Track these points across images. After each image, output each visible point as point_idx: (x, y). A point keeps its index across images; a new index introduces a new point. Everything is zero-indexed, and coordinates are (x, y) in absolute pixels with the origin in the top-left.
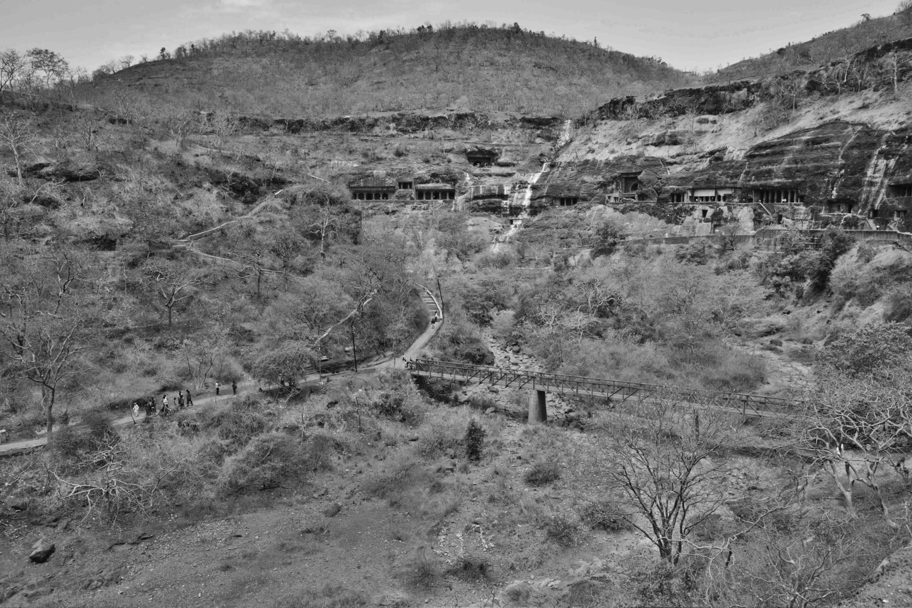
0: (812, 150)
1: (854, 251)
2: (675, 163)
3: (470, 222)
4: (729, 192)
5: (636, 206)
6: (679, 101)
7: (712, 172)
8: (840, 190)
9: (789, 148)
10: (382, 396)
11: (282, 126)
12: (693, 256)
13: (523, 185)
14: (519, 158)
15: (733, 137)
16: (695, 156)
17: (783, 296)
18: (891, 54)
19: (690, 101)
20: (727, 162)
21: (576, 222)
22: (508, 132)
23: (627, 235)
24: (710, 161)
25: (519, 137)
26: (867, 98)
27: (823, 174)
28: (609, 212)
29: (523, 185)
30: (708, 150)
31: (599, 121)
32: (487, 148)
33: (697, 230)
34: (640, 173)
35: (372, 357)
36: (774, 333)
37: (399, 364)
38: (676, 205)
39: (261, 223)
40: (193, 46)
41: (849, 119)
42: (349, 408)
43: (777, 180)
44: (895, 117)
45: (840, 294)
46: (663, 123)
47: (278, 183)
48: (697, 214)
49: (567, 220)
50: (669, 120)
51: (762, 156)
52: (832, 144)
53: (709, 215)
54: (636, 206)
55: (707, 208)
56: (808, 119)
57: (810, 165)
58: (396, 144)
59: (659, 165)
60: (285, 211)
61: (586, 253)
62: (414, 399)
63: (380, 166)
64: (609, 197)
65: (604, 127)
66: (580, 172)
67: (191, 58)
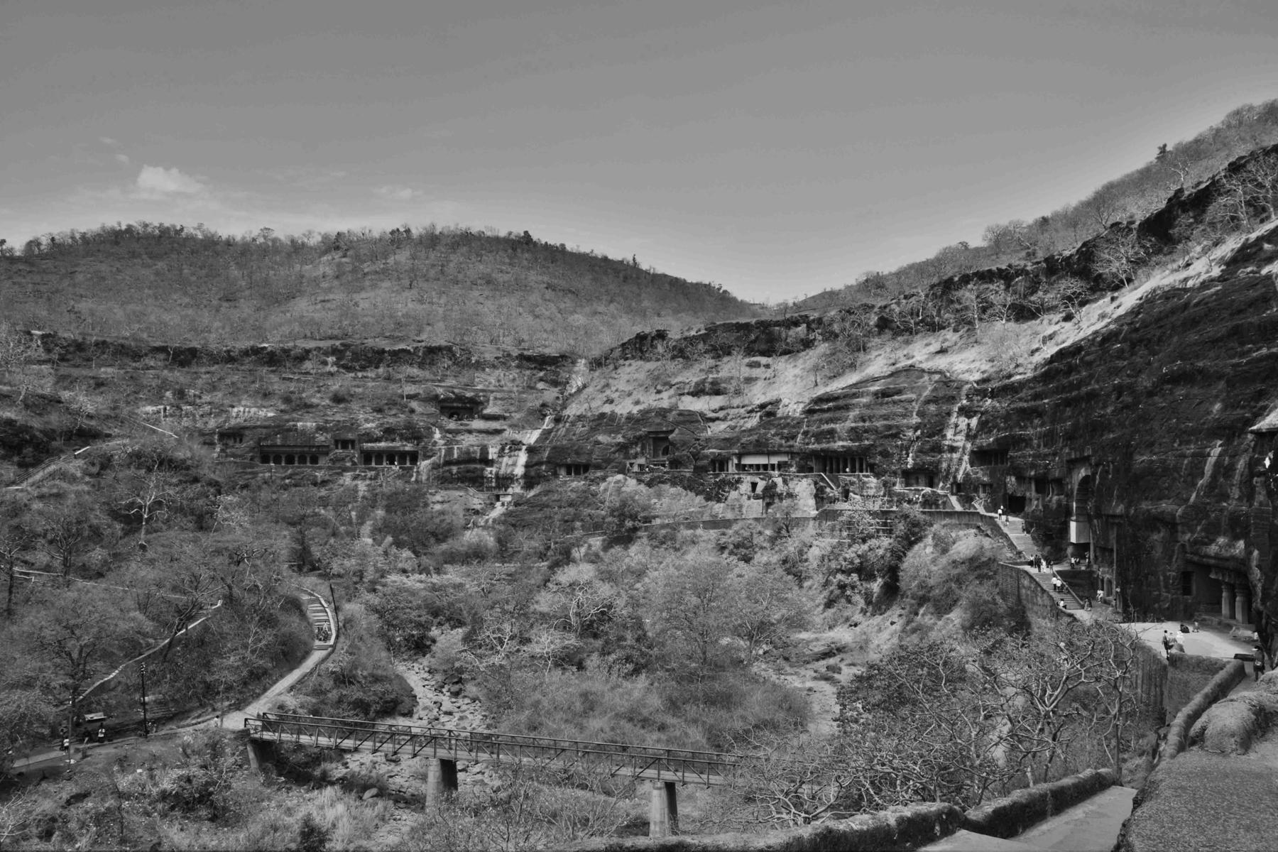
0: (881, 404)
1: (929, 540)
2: (718, 419)
3: (438, 498)
4: (784, 459)
5: (667, 476)
6: (723, 338)
7: (762, 431)
9: (855, 401)
10: (180, 778)
11: (162, 356)
12: (737, 546)
13: (516, 445)
14: (513, 409)
15: (790, 385)
16: (742, 411)
17: (849, 602)
18: (969, 286)
19: (738, 339)
21: (587, 498)
22: (499, 372)
23: (654, 517)
25: (514, 380)
26: (946, 340)
27: (896, 436)
28: (631, 484)
29: (516, 445)
30: (758, 402)
31: (621, 362)
32: (469, 395)
33: (744, 510)
34: (672, 431)
35: (190, 711)
36: (834, 655)
37: (234, 722)
38: (717, 476)
39: (41, 497)
40: (53, 239)
41: (925, 366)
42: (110, 802)
43: (841, 443)
44: (977, 364)
45: (912, 598)
46: (703, 367)
47: (86, 436)
48: (745, 487)
49: (573, 496)
50: (711, 362)
51: (823, 411)
53: (759, 490)
54: (667, 476)
55: (757, 480)
56: (878, 363)
57: (879, 424)
58: (335, 386)
59: (698, 421)
60: (87, 479)
61: (596, 542)
62: (246, 782)
63: (307, 416)
64: (631, 464)
65: (628, 369)
66: (594, 430)
67: (43, 256)
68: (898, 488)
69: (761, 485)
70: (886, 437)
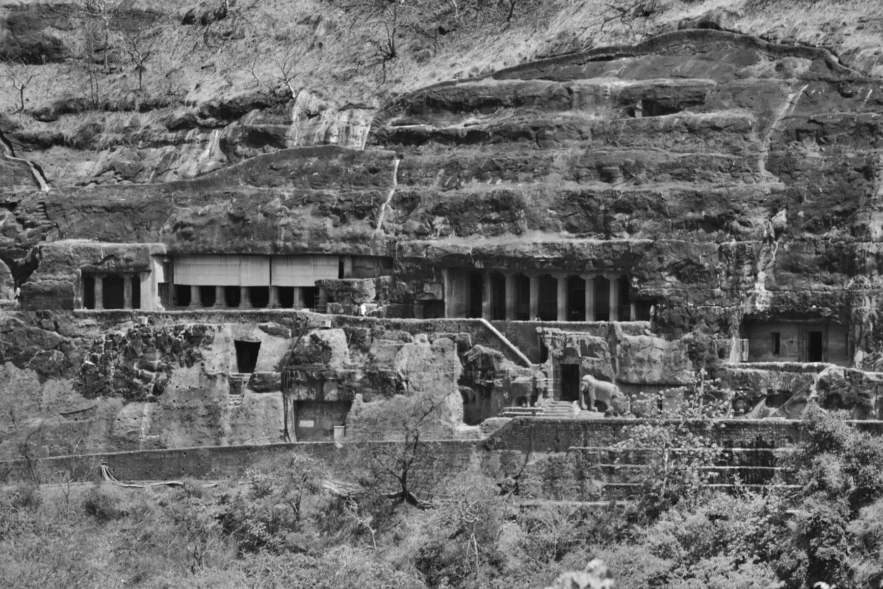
0: (652, 132)
2: (59, 141)
4: (329, 273)
7: (249, 190)
8: (781, 281)
16: (145, 119)
20: (304, 153)
24: (224, 144)
38: (116, 319)
41: (745, 26)
48: (219, 357)
52: (709, 116)
57: (667, 189)
68: (735, 360)
69: (272, 352)
70: (692, 225)
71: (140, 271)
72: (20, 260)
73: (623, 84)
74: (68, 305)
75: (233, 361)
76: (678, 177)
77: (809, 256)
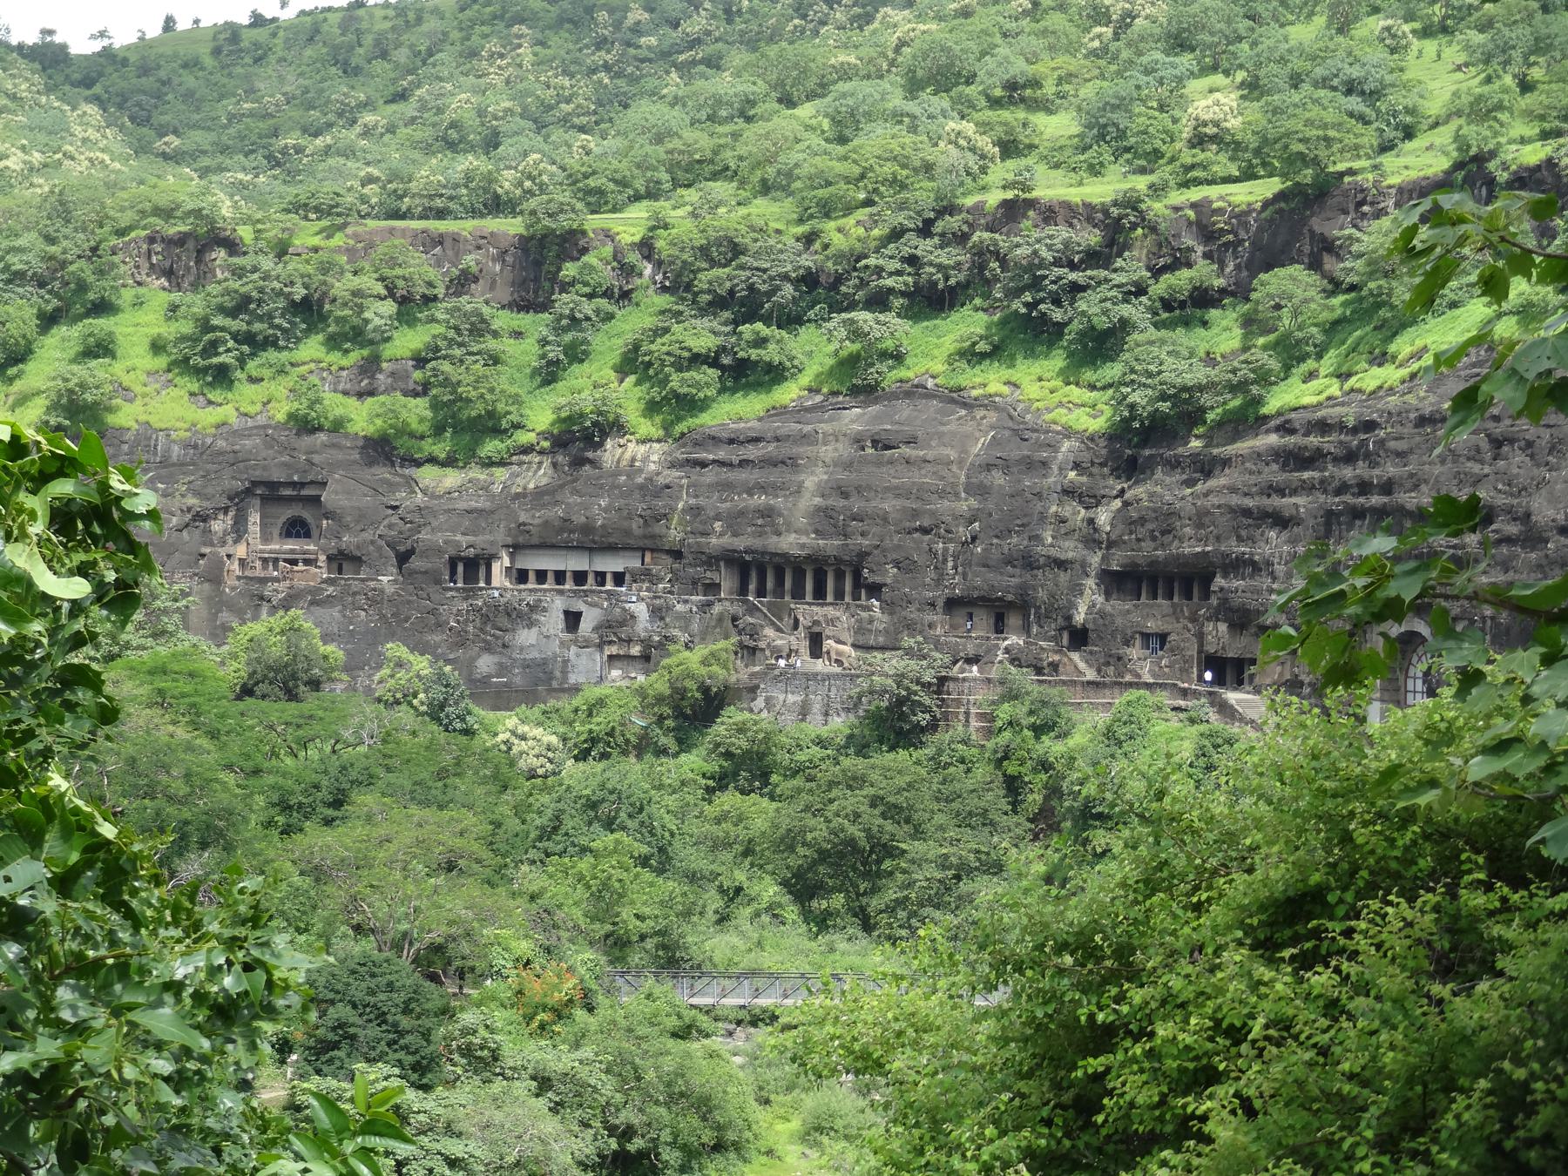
48: (554, 621)
53: (586, 626)
57: (889, 505)
71: (489, 560)
72: (402, 549)
73: (857, 427)
74: (438, 582)
75: (561, 625)
76: (898, 496)
77: (995, 555)
